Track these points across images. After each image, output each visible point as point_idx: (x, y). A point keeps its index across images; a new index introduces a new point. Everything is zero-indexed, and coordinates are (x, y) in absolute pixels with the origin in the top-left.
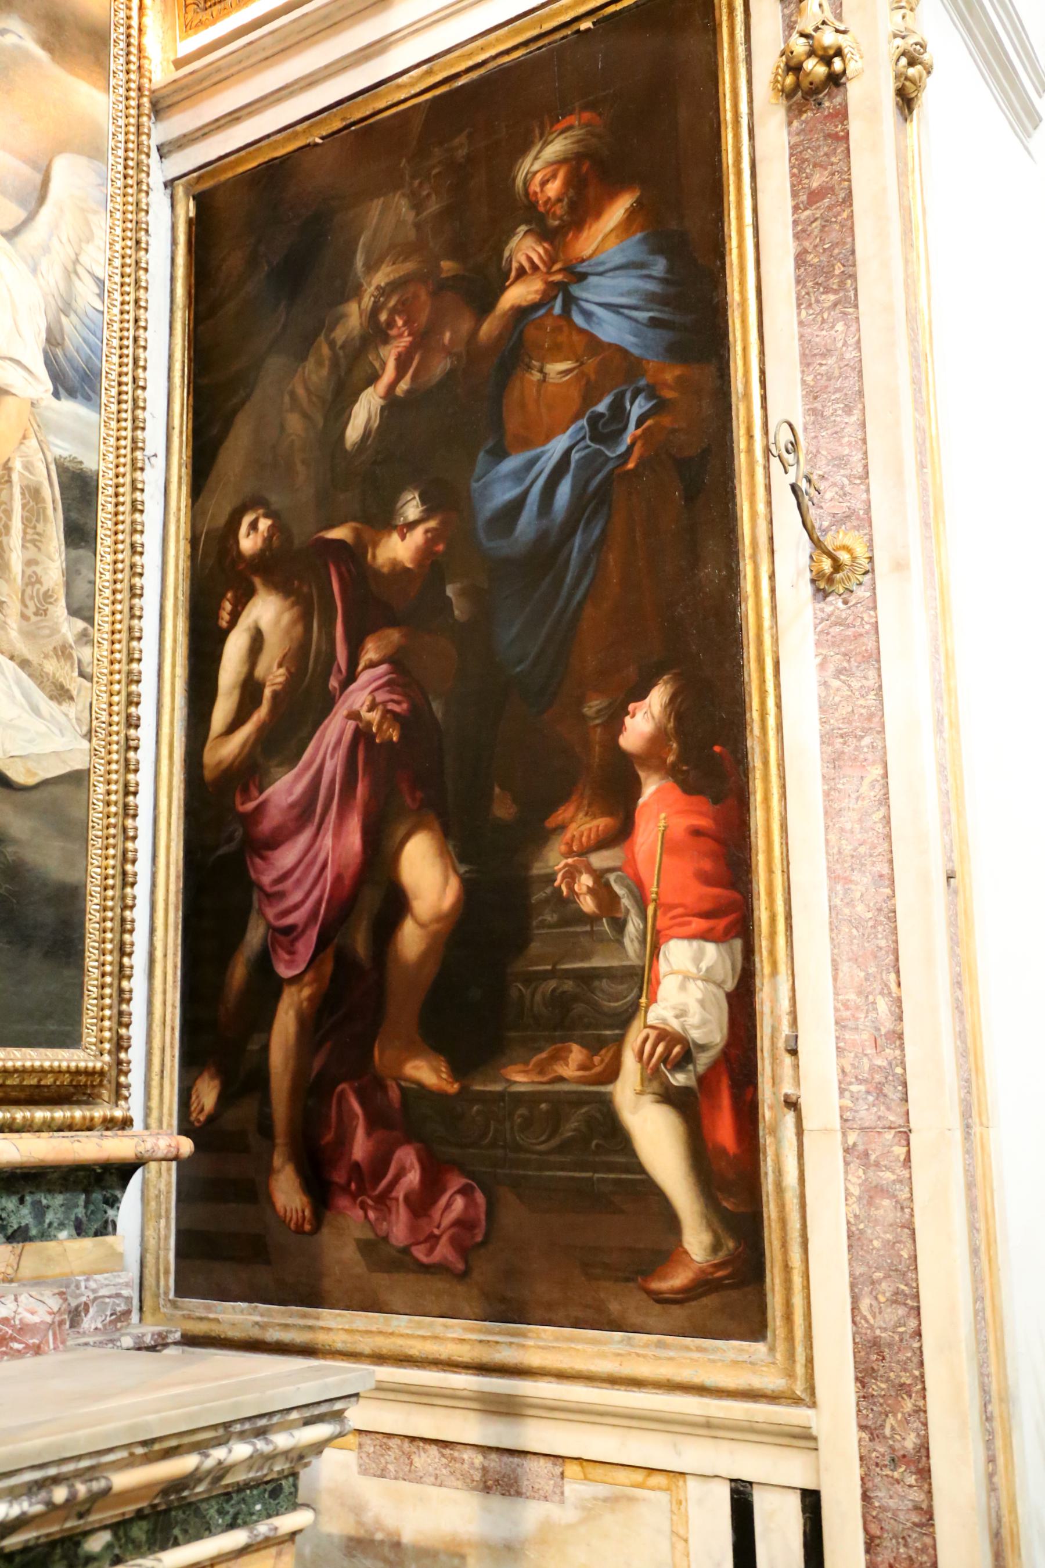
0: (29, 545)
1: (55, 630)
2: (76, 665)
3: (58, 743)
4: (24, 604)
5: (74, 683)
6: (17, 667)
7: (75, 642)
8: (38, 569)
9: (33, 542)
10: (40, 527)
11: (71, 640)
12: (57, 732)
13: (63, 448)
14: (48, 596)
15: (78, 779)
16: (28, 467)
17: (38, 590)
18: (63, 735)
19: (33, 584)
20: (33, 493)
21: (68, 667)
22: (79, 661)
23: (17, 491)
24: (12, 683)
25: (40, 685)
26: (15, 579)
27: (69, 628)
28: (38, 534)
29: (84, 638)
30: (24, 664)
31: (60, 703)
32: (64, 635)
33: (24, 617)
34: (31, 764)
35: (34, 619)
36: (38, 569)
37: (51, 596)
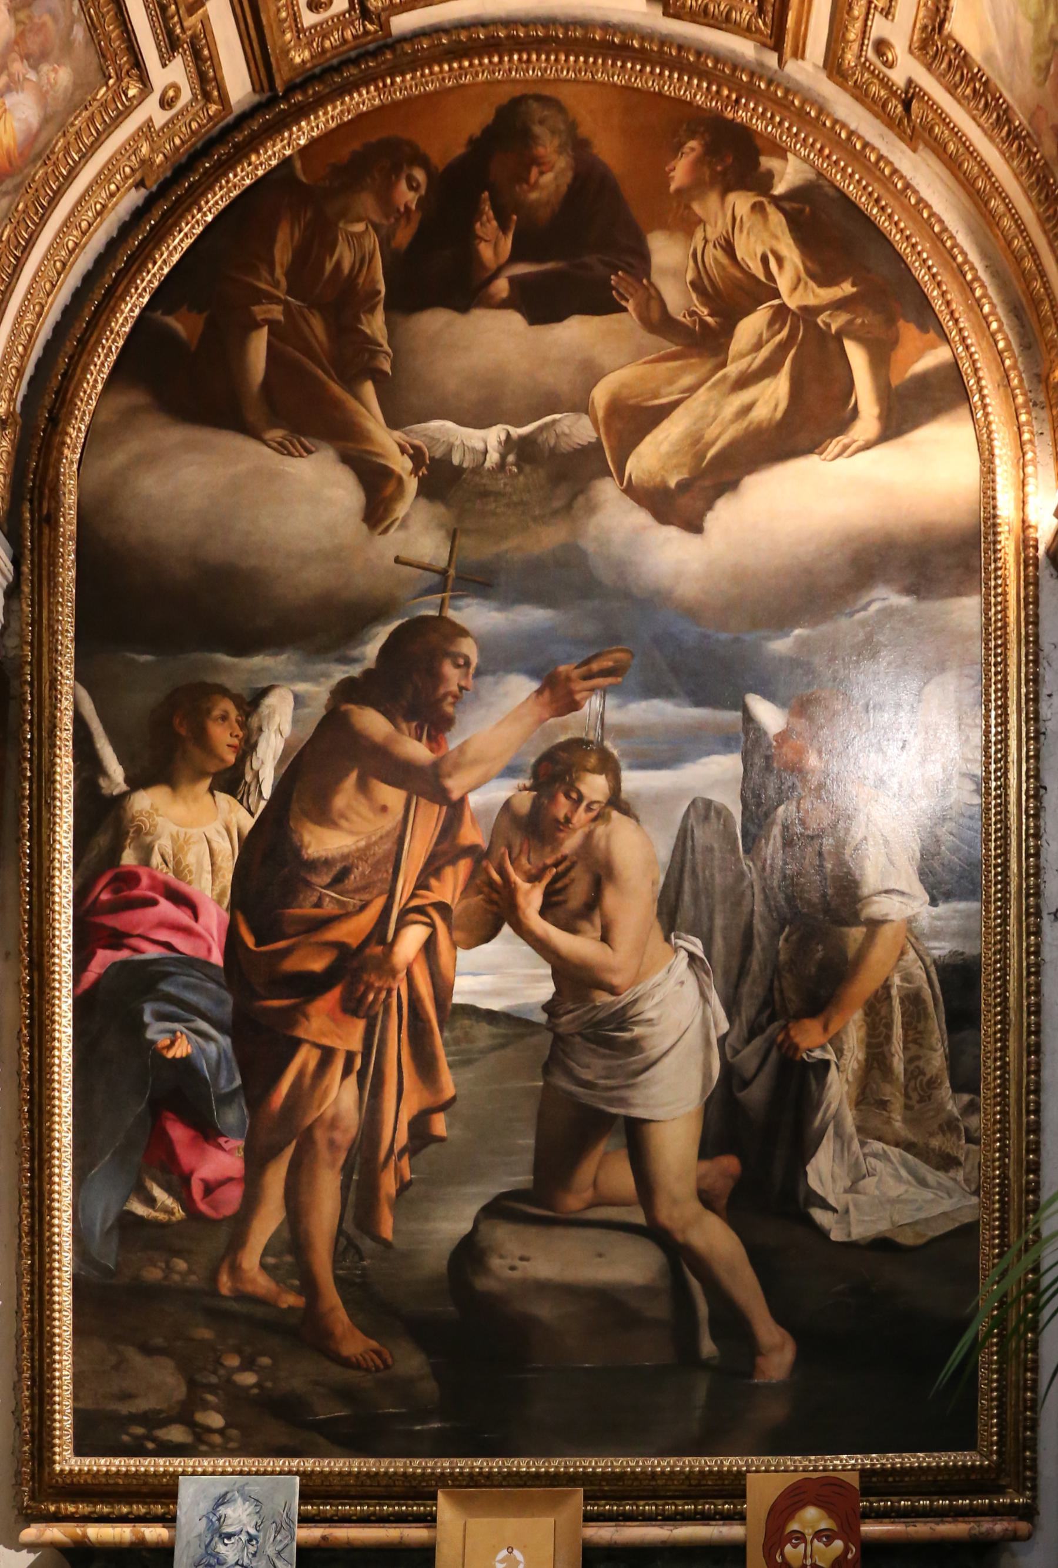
0: (910, 1045)
1: (941, 1108)
2: (963, 1134)
3: (947, 1205)
4: (907, 1096)
5: (961, 1148)
6: (902, 1151)
7: (961, 1115)
8: (921, 1063)
9: (915, 1041)
10: (921, 1027)
11: (956, 1112)
12: (945, 1196)
13: (941, 948)
14: (933, 1084)
15: (968, 1232)
16: (907, 978)
17: (921, 1081)
18: (951, 1197)
19: (916, 1078)
20: (913, 1001)
21: (954, 1138)
22: (967, 1129)
23: (896, 1003)
24: (898, 1166)
25: (927, 1161)
26: (898, 1079)
27: (951, 1103)
28: (920, 1033)
29: (971, 1108)
30: (909, 1147)
31: (947, 1171)
32: (950, 1111)
33: (907, 1107)
34: (918, 1228)
35: (917, 1106)
36: (921, 1063)
37: (934, 1082)
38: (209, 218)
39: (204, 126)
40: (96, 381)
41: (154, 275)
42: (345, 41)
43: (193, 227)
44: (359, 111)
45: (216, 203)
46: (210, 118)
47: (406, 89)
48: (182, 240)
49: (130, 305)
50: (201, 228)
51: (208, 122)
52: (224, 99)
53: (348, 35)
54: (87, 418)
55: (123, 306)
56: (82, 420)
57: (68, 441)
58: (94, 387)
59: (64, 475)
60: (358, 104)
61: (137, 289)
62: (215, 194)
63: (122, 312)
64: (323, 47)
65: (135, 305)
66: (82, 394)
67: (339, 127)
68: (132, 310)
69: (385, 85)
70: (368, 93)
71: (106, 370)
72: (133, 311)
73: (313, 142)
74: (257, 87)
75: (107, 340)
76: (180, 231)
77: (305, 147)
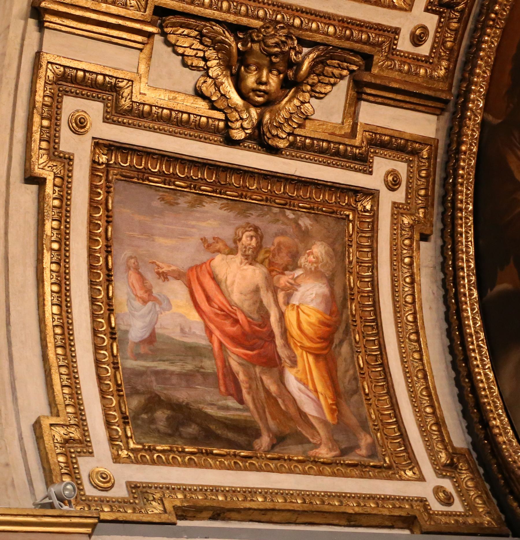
38: (471, 208)
39: (429, 166)
40: (486, 375)
41: (468, 275)
42: (456, 30)
43: (466, 223)
44: (495, 49)
45: (467, 195)
46: (428, 158)
47: (506, 5)
48: (467, 238)
49: (469, 309)
50: (471, 218)
51: (429, 162)
52: (424, 141)
53: (454, 25)
54: (499, 403)
55: (465, 314)
56: (496, 407)
57: (497, 431)
58: (488, 379)
59: (510, 456)
60: (490, 47)
61: (465, 295)
62: (462, 192)
63: (468, 317)
64: (448, 49)
65: (472, 305)
66: (483, 393)
67: (492, 72)
68: (472, 310)
69: (493, 20)
70: (489, 36)
71: (487, 361)
72: (474, 309)
73: (487, 98)
74: (438, 113)
75: (473, 344)
76: (461, 235)
77: (485, 105)
